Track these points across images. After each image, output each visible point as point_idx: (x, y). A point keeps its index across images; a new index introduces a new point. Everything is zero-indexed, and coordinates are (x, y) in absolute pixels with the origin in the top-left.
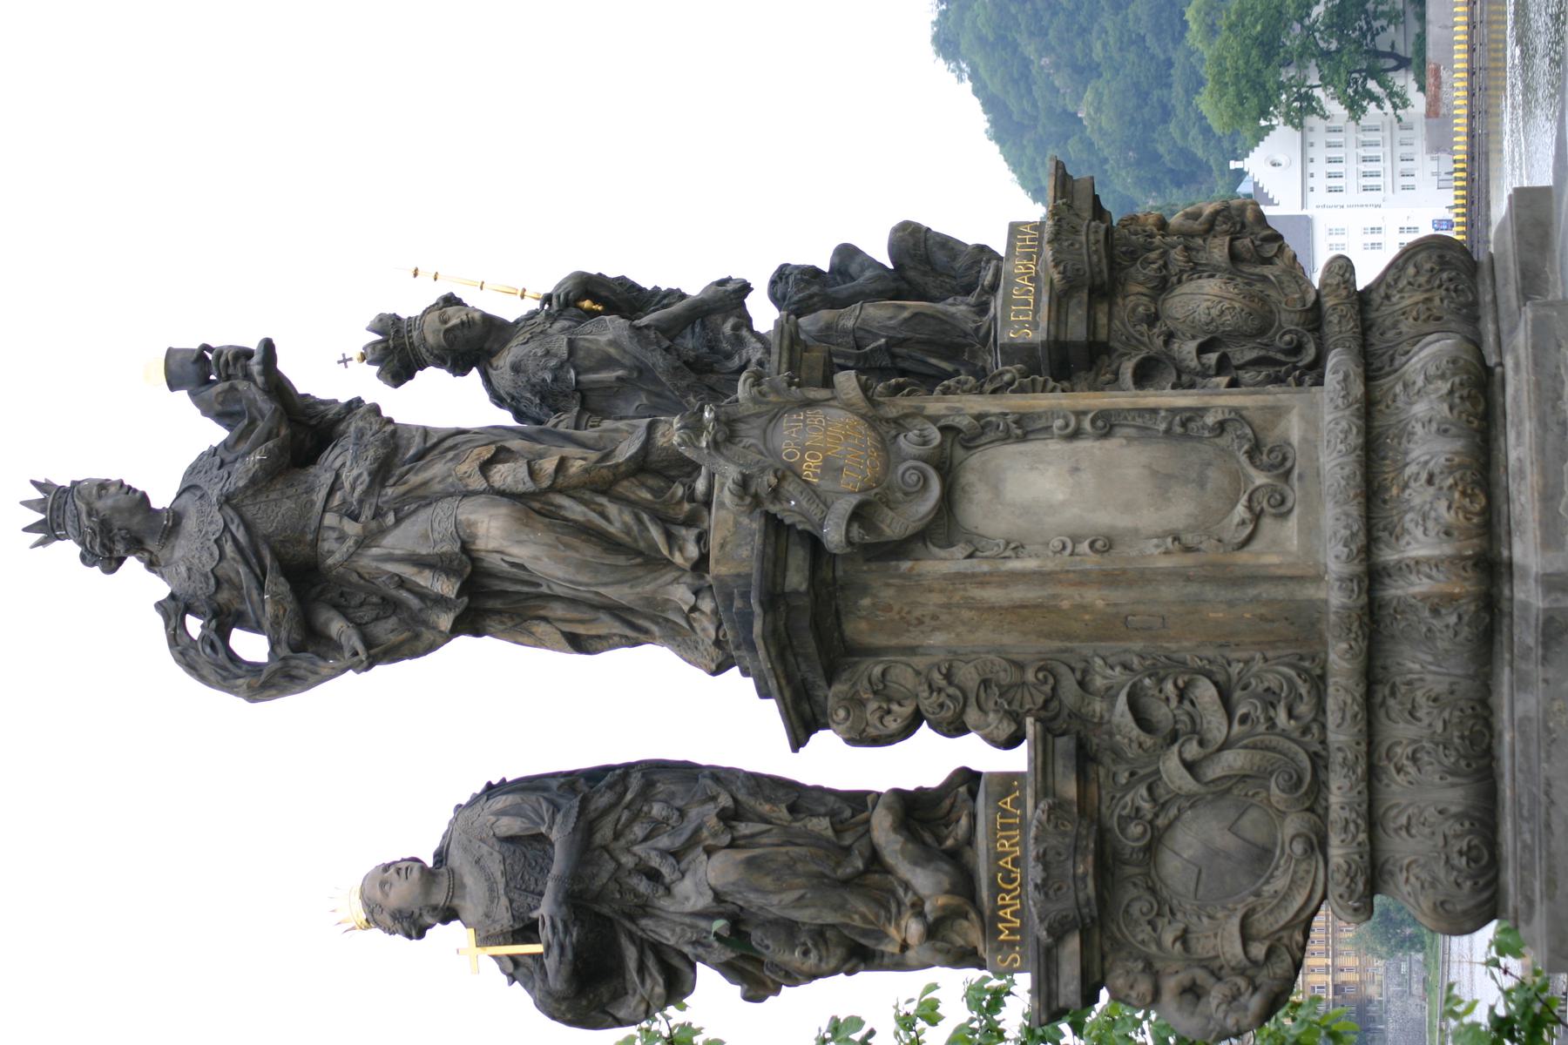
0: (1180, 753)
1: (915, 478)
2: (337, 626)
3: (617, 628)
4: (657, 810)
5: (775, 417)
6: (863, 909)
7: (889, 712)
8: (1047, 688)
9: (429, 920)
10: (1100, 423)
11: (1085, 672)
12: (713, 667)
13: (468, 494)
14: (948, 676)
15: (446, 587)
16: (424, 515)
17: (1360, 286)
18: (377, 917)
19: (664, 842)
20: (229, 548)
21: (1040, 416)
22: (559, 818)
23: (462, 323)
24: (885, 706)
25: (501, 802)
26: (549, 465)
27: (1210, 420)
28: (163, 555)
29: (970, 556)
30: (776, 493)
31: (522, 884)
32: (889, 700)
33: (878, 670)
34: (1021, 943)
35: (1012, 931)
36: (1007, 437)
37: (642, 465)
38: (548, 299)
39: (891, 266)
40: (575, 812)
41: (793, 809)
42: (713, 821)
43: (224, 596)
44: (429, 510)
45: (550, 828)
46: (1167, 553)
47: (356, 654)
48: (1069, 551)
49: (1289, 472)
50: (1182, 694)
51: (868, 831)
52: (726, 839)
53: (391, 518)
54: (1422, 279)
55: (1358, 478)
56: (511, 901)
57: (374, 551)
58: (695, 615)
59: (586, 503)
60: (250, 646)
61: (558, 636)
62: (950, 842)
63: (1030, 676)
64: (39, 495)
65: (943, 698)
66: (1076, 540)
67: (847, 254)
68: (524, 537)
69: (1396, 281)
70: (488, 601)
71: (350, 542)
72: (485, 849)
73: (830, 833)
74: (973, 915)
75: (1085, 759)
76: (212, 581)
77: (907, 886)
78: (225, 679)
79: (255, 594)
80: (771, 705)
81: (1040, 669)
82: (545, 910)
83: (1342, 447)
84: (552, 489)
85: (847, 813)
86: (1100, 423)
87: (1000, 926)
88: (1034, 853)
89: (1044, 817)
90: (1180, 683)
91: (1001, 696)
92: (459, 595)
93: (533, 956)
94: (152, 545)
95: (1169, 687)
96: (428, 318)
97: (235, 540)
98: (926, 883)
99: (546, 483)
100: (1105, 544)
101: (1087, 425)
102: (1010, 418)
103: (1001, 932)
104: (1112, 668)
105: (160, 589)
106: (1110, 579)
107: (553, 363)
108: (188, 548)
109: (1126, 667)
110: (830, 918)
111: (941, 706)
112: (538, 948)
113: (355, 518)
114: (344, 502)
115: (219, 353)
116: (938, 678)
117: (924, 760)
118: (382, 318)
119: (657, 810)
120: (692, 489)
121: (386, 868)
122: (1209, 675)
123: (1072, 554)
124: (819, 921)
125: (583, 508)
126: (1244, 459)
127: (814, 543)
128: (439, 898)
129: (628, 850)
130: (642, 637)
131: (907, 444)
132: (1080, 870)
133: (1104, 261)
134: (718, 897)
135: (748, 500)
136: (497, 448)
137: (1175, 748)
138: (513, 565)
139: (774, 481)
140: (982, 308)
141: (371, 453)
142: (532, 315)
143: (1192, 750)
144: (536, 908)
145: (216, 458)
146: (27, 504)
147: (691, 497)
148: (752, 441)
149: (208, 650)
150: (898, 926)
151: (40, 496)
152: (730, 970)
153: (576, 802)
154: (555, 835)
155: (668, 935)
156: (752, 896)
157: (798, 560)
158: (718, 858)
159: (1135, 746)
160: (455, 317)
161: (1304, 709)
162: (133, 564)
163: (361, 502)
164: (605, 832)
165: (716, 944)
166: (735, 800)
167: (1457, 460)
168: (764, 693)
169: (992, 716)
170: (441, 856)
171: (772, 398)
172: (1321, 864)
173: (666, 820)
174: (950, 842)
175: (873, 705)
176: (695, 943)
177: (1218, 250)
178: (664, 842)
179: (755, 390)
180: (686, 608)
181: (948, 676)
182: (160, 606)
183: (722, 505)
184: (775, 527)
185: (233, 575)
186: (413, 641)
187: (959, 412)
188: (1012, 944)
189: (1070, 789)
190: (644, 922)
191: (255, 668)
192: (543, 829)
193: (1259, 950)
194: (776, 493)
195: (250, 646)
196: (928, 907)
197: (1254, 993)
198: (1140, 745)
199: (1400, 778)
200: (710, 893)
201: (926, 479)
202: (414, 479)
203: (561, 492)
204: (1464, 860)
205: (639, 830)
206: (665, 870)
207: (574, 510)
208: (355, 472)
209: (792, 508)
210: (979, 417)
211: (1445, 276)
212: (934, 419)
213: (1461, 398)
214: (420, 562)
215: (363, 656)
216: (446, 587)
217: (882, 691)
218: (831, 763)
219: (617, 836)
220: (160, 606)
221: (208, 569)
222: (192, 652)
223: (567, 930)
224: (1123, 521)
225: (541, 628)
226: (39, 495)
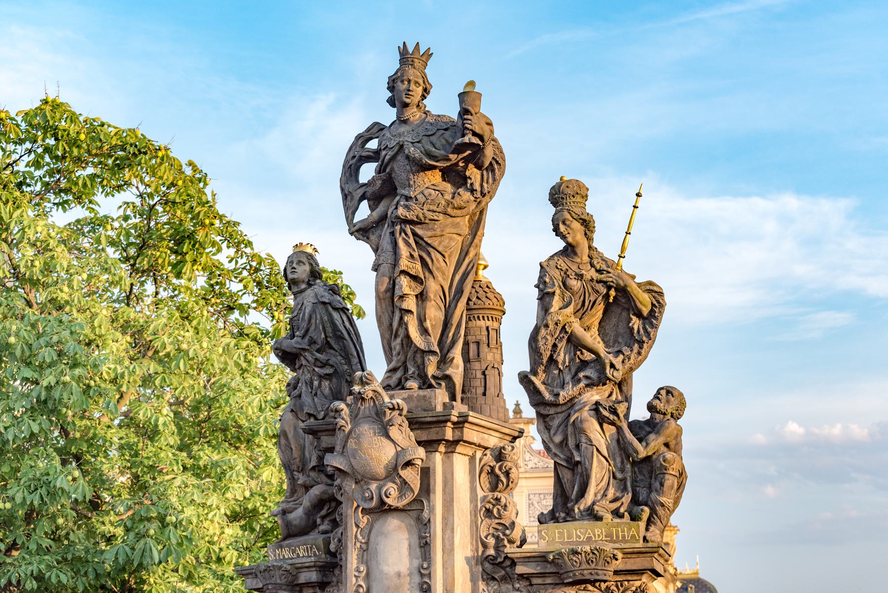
4: (316, 383)
10: (425, 586)
36: (421, 537)
86: (425, 586)
123: (355, 576)
133: (571, 580)
189: (303, 578)
195: (368, 172)
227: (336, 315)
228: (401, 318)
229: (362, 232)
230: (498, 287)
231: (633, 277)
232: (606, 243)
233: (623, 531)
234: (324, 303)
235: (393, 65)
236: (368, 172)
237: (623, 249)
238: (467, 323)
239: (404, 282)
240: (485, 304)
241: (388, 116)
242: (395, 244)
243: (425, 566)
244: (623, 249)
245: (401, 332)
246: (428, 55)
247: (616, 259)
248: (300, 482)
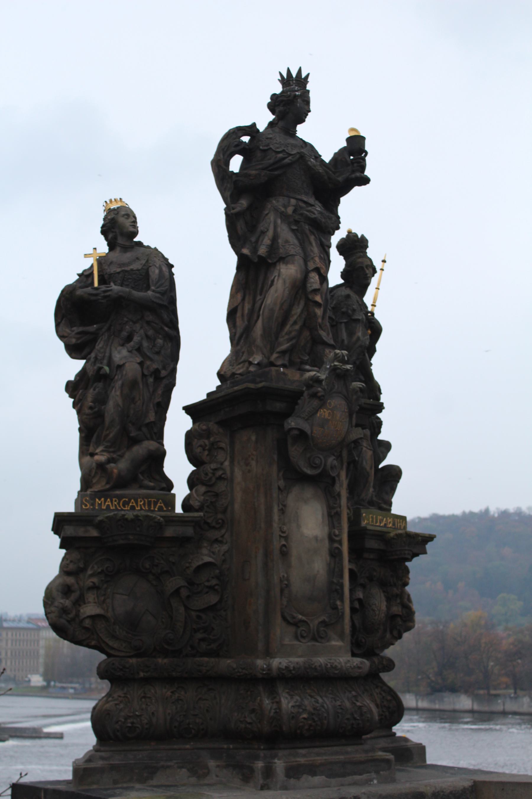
0: (184, 587)
1: (317, 462)
2: (244, 203)
3: (239, 330)
5: (346, 399)
6: (111, 435)
7: (204, 450)
8: (214, 524)
9: (110, 236)
10: (337, 551)
11: (221, 542)
12: (222, 373)
13: (306, 261)
14: (220, 478)
15: (262, 251)
16: (296, 242)
17: (382, 675)
18: (112, 213)
19: (145, 344)
20: (281, 155)
21: (340, 523)
22: (158, 295)
23: (367, 274)
24: (207, 448)
25: (165, 269)
26: (318, 298)
27: (338, 603)
28: (277, 129)
29: (279, 488)
30: (314, 395)
31: (126, 277)
32: (209, 450)
33: (223, 445)
34: (94, 509)
35: (100, 505)
36: (330, 508)
37: (317, 341)
38: (373, 314)
39: (381, 466)
40: (160, 302)
41: (159, 404)
42: (155, 366)
43: (259, 154)
44: (298, 244)
45: (153, 291)
46: (281, 581)
47: (233, 209)
48: (282, 535)
49: (316, 640)
50: (212, 588)
51: (148, 439)
52: (146, 372)
53: (295, 227)
54: (385, 703)
55: (315, 674)
56: (119, 273)
57: (279, 221)
58: (247, 364)
59: (300, 316)
60: (236, 163)
61: (235, 305)
62: (141, 477)
63: (220, 516)
64: (303, 76)
65: (210, 475)
66: (286, 538)
67: (387, 446)
68: (287, 285)
69: (384, 691)
70: (251, 275)
71: (283, 209)
72: (144, 262)
73: (147, 421)
74: (108, 486)
75: (182, 541)
76: (266, 148)
77: (122, 456)
78: (223, 149)
79: (261, 166)
80: (204, 397)
81: (223, 521)
82: (115, 288)
83: (329, 666)
84: (308, 300)
85: (155, 430)
86: (337, 551)
87: (103, 499)
88: (139, 514)
89: (156, 520)
90: (216, 587)
91: (211, 502)
92: (260, 257)
93: (93, 283)
94: (281, 124)
95: (214, 582)
96: (369, 261)
97: (284, 159)
98: (122, 466)
99: (310, 297)
100: (285, 553)
101: (336, 545)
102: (339, 509)
103: (100, 499)
104: (223, 555)
105: (262, 127)
106: (267, 554)
107: (350, 312)
108: (279, 138)
109: (224, 561)
110: (107, 420)
111: (206, 474)
112: (96, 284)
113: (295, 211)
114: (301, 208)
115: (364, 160)
116: (220, 473)
117: (178, 468)
118: (367, 241)
119: (160, 341)
120: (306, 364)
121: (135, 217)
122: (220, 601)
123: (280, 536)
124: (106, 414)
125: (298, 314)
126: (321, 619)
127: (287, 415)
128: (121, 240)
129: (141, 328)
130: (235, 342)
131: (331, 460)
132: (131, 537)
134: (120, 367)
135: (311, 382)
136: (324, 279)
137: (186, 584)
138: (273, 281)
139: (319, 394)
140: (371, 503)
141: (323, 220)
142: (367, 307)
143: (184, 593)
144: (115, 285)
145: (317, 156)
146: (300, 71)
147: (303, 362)
148: (336, 387)
149: (236, 143)
150: (103, 451)
151: (303, 76)
152: (82, 375)
153: (165, 303)
154: (150, 293)
155: (101, 345)
156: (120, 382)
157: (279, 406)
158: (137, 367)
159: (188, 565)
160: (369, 271)
161: (204, 646)
162: (271, 117)
163: (302, 214)
164: (150, 317)
165: (95, 368)
166: (164, 378)
167: (325, 722)
168: (209, 395)
169: (202, 498)
170: (140, 244)
171: (355, 397)
172: (128, 654)
173: (154, 346)
174: (141, 477)
175: (207, 442)
176: (96, 358)
177: (396, 609)
178: (145, 344)
179: (358, 389)
180: (251, 360)
181: (220, 478)
182: (254, 125)
183: (302, 375)
184: (298, 395)
185: (268, 157)
186: (236, 239)
187: (341, 486)
188: (93, 504)
190: (106, 334)
191: (228, 164)
192: (153, 288)
193: (87, 623)
194: (314, 395)
195: (236, 163)
196: (112, 465)
197: (68, 621)
198: (188, 567)
199: (169, 693)
200: (122, 363)
201: (315, 468)
202: (312, 238)
203: (306, 305)
204: (130, 725)
205: (151, 333)
206: (132, 343)
207: (297, 310)
208: (316, 212)
209: (306, 405)
210: (339, 495)
211: (387, 714)
212: (338, 475)
213: (353, 724)
214: (275, 239)
215: (232, 211)
216: (262, 251)
217: (214, 447)
218: (177, 426)
219: (148, 323)
220: (254, 125)
221: (271, 146)
222: (234, 136)
223: (105, 297)
224: (294, 561)
225: (239, 297)
226: (303, 76)
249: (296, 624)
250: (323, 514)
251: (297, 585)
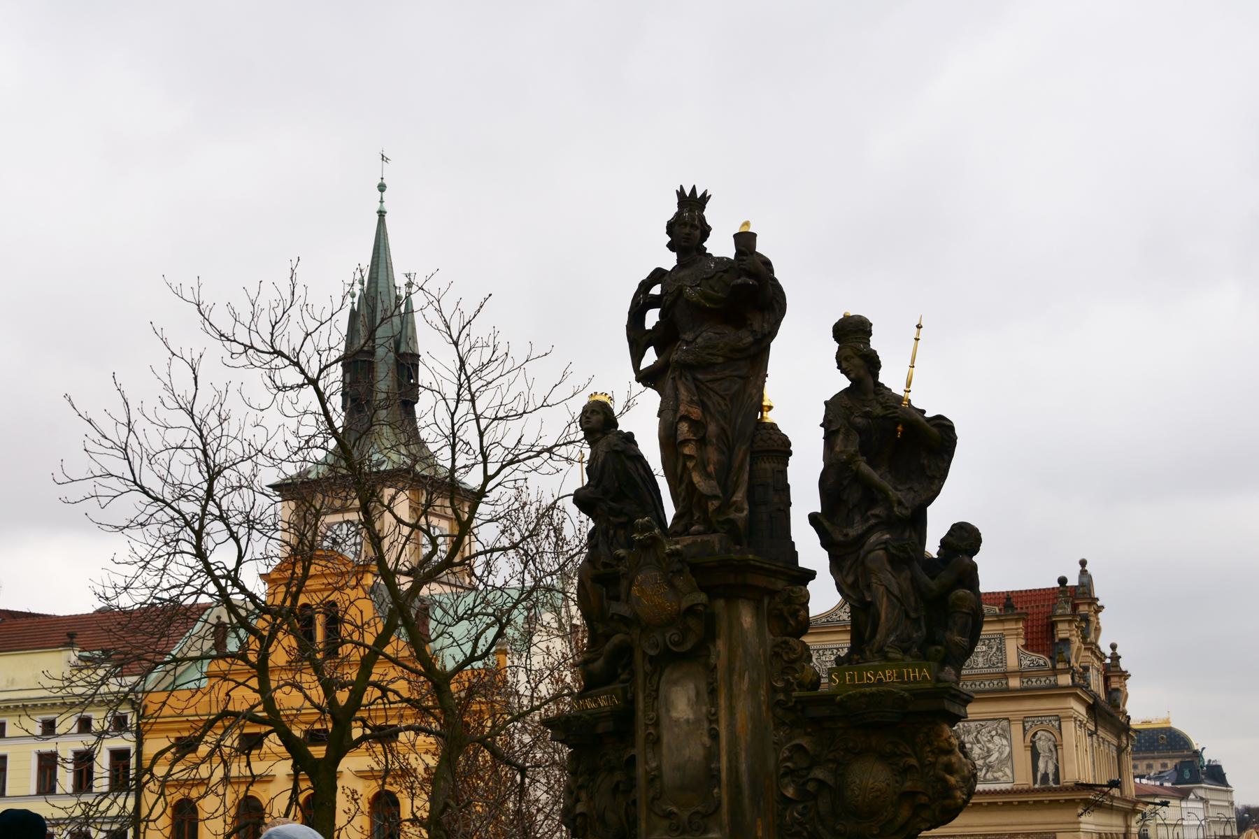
4: (612, 532)
46: (647, 773)
62: (620, 671)
66: (657, 724)
100: (656, 742)
123: (647, 725)
143: (621, 787)
187: (718, 657)
189: (600, 729)
195: (652, 318)
224: (665, 750)
227: (629, 464)
228: (685, 465)
229: (647, 378)
230: (784, 429)
231: (924, 412)
232: (891, 377)
233: (914, 672)
234: (617, 452)
235: (671, 209)
236: (652, 318)
237: (909, 385)
238: (751, 465)
239: (684, 427)
240: (778, 448)
241: (669, 261)
242: (676, 389)
243: (713, 710)
244: (909, 385)
245: (686, 480)
246: (705, 198)
247: (902, 393)
248: (600, 631)
249: (669, 815)
250: (698, 694)
251: (669, 776)
